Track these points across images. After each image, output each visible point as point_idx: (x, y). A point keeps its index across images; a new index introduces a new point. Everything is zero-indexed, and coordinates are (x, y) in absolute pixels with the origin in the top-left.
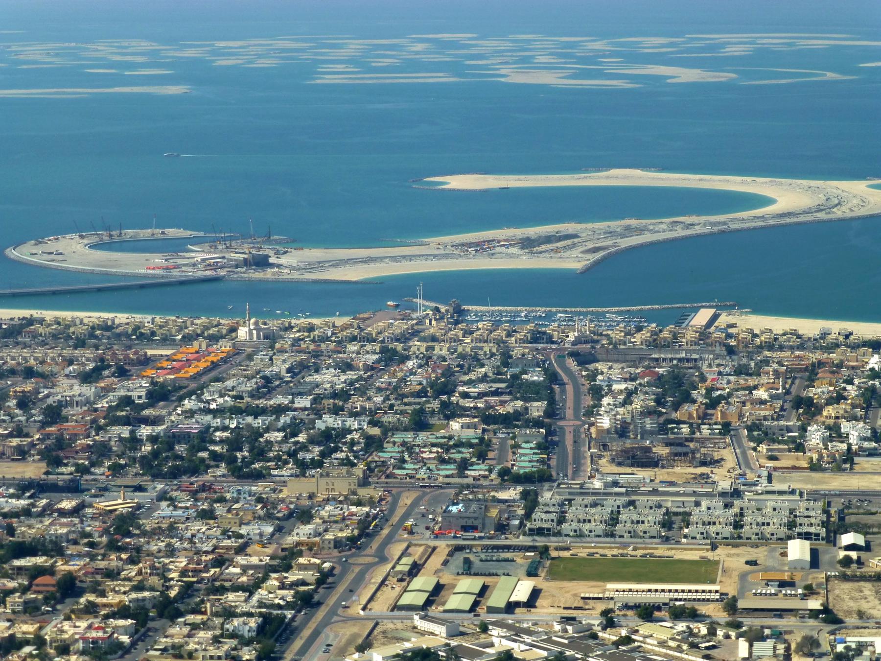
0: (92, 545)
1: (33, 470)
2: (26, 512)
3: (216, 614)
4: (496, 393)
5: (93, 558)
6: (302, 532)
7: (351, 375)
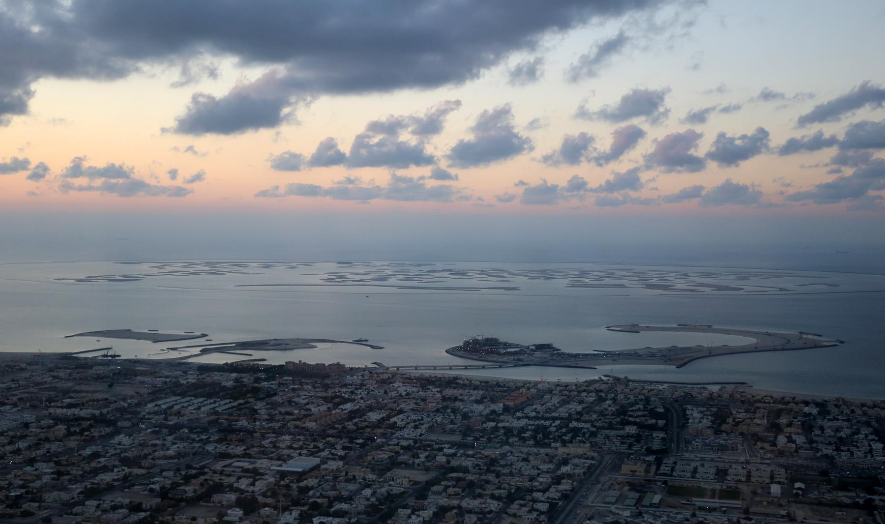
0: (480, 469)
1: (457, 438)
2: (454, 455)
3: (530, 501)
4: (643, 416)
5: (480, 474)
6: (565, 469)
7: (584, 405)
